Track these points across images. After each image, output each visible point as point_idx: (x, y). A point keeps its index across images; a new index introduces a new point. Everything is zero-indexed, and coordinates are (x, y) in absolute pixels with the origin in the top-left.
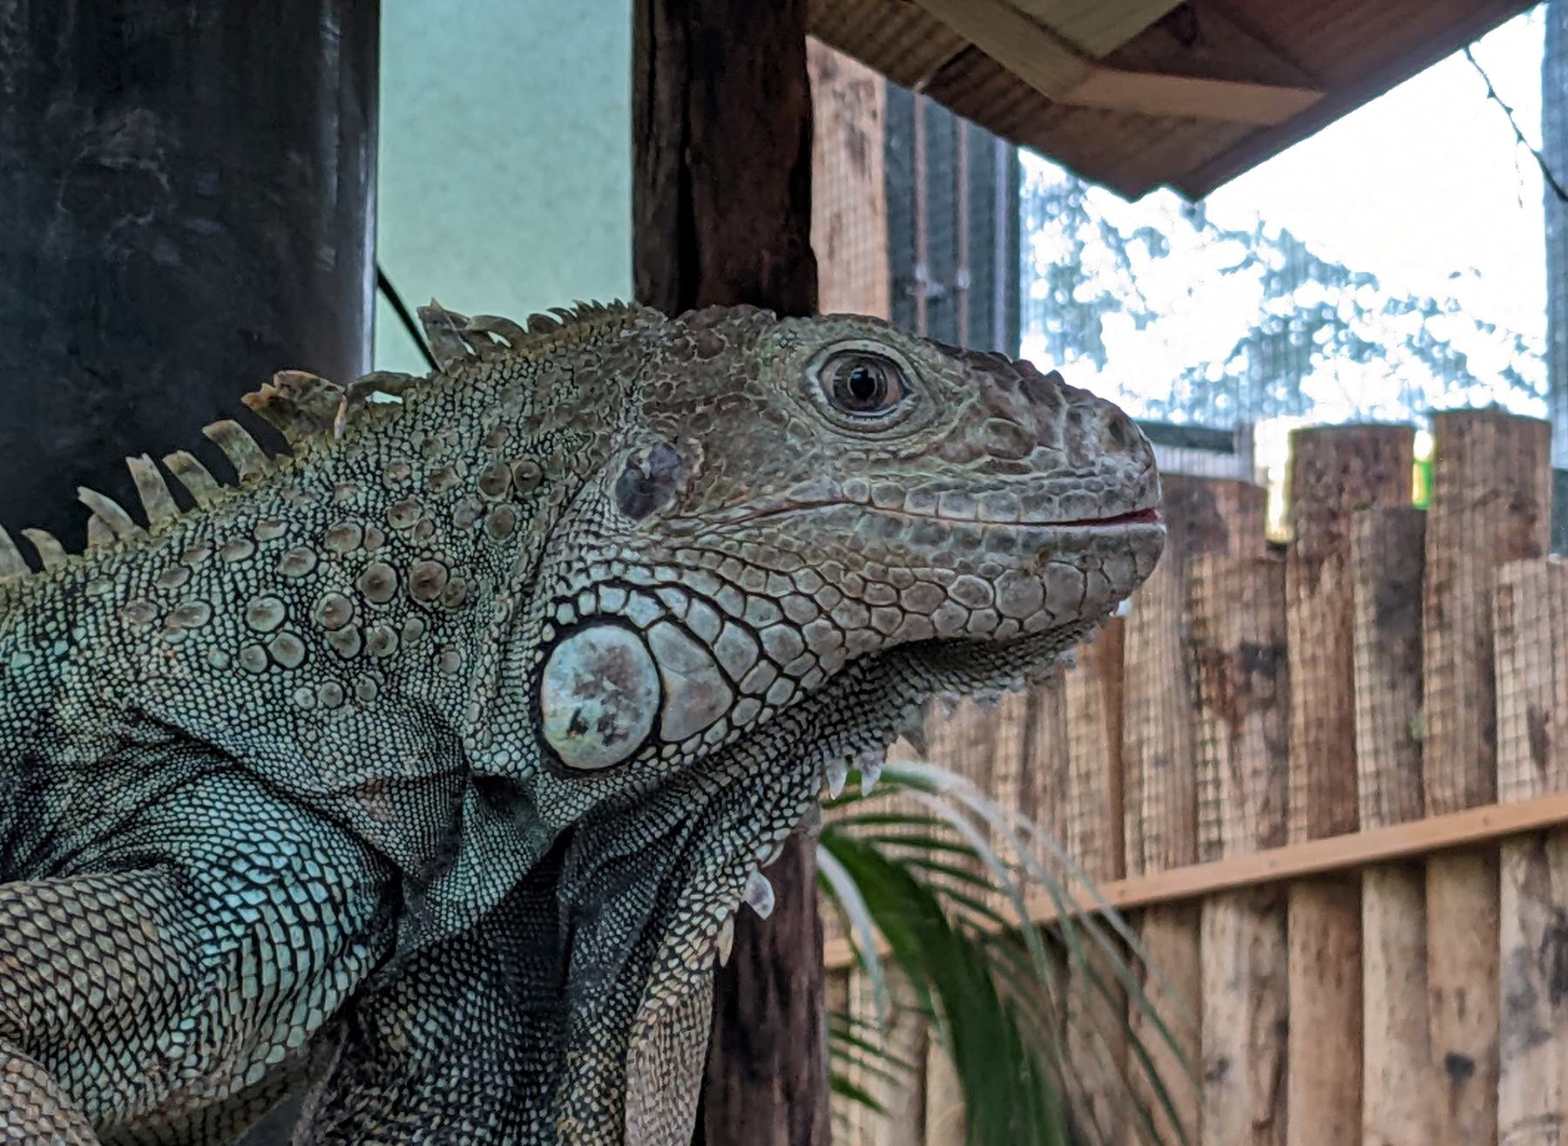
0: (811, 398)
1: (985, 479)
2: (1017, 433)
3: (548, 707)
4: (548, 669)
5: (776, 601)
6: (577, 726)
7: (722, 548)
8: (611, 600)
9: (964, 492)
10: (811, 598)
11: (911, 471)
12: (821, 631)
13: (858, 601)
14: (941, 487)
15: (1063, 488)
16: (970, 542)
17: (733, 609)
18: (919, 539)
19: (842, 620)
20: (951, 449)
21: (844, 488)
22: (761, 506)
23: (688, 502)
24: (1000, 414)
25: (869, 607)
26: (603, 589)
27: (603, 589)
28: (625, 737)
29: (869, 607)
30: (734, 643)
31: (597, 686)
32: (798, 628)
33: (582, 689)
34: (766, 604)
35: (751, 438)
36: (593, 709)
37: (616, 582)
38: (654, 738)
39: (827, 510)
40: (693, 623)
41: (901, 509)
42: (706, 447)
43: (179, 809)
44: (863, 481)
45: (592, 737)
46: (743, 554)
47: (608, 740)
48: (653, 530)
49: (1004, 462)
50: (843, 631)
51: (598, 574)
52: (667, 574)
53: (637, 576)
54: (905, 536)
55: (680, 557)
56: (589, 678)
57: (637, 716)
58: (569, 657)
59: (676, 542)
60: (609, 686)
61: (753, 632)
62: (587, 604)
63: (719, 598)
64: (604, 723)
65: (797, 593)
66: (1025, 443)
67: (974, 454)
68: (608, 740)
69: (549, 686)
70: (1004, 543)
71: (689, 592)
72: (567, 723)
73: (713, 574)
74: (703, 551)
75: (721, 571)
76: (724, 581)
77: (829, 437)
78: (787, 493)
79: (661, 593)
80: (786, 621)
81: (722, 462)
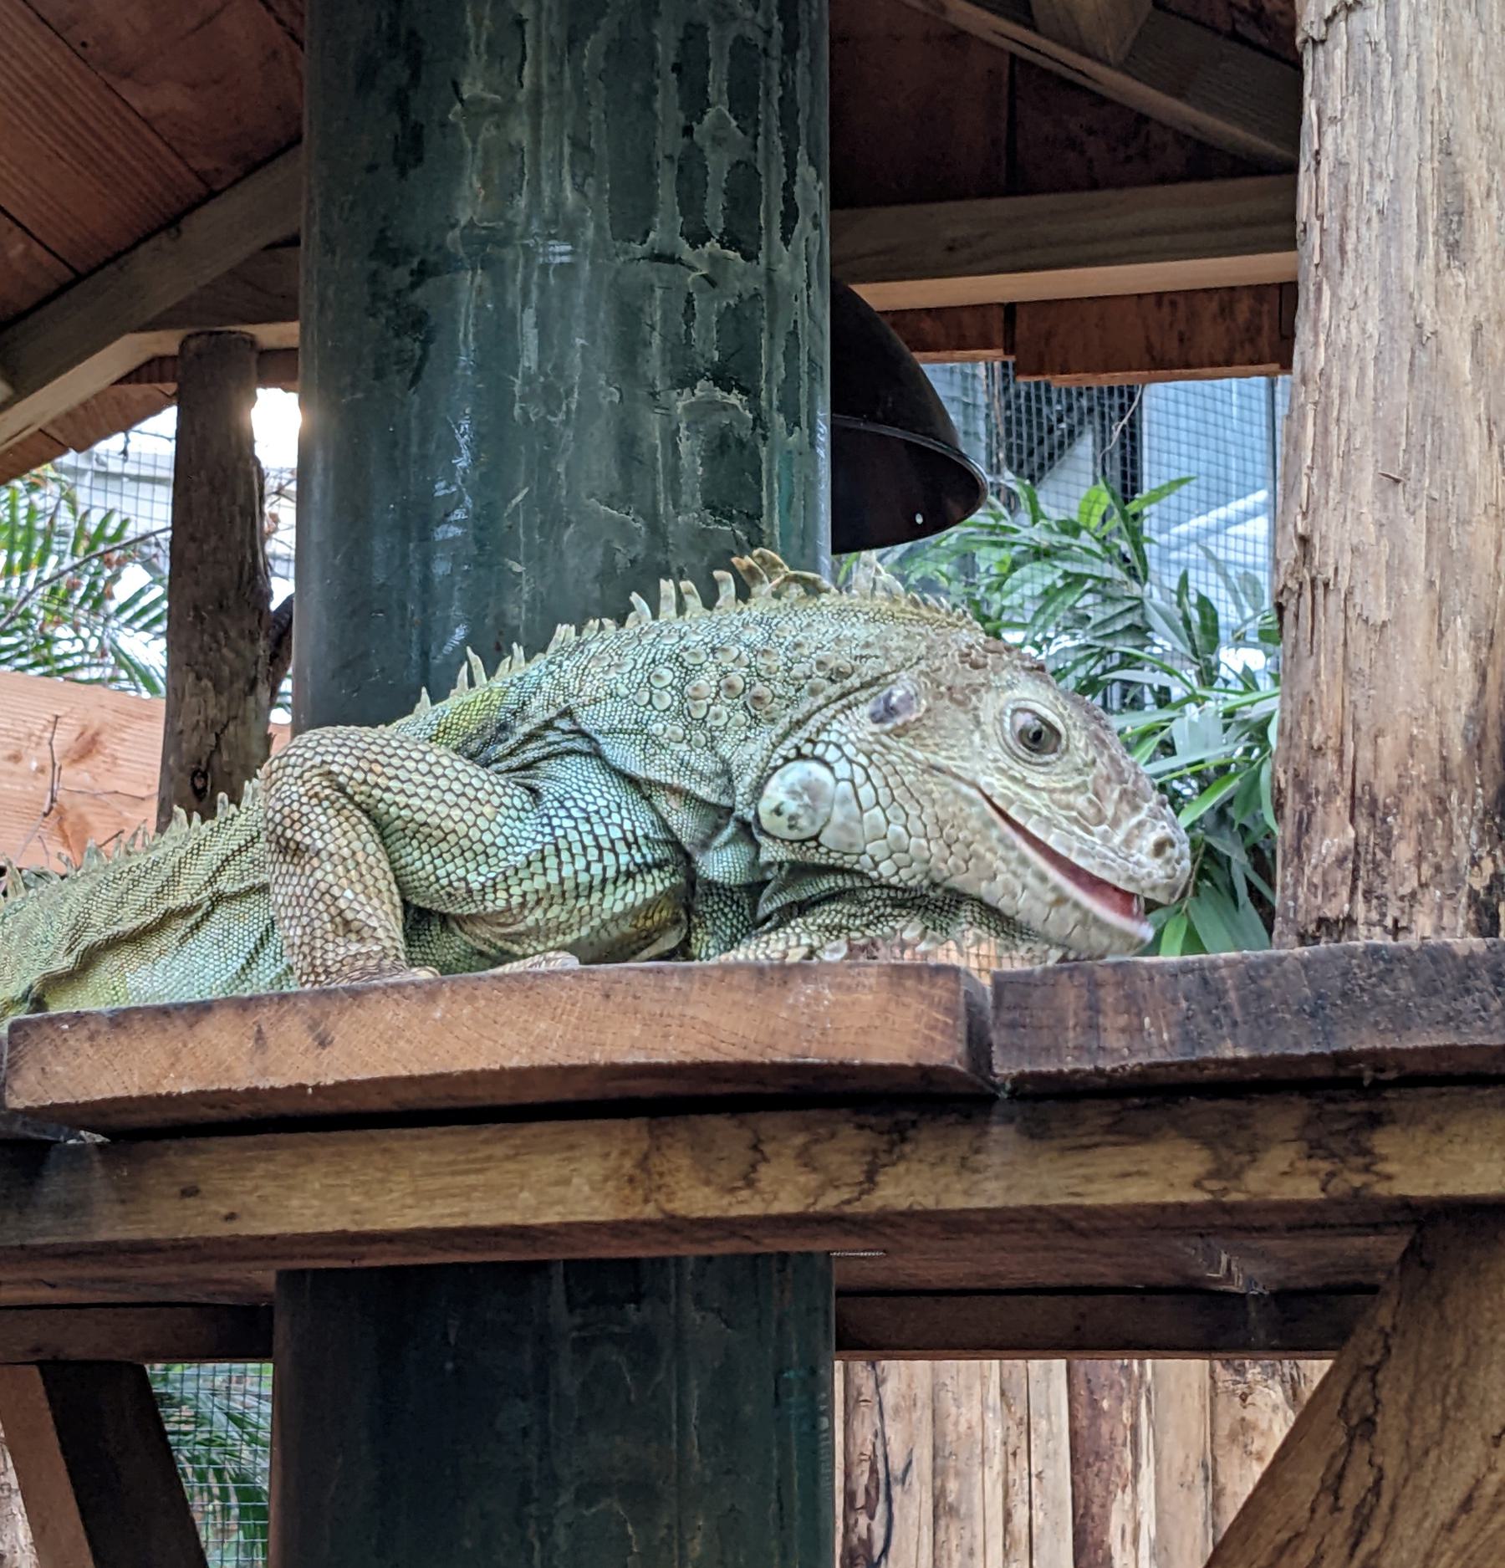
0: (1001, 721)
3: (768, 791)
4: (780, 772)
6: (778, 811)
7: (898, 768)
17: (884, 801)
21: (983, 780)
22: (933, 759)
23: (899, 732)
31: (800, 796)
33: (793, 793)
35: (955, 720)
36: (791, 806)
40: (861, 792)
42: (928, 710)
43: (553, 767)
45: (783, 821)
46: (907, 779)
47: (791, 827)
48: (873, 734)
52: (863, 760)
55: (875, 757)
56: (798, 789)
57: (813, 823)
58: (796, 772)
59: (878, 748)
60: (806, 798)
63: (880, 791)
64: (792, 818)
68: (791, 827)
69: (774, 781)
71: (868, 778)
72: (773, 805)
73: (885, 778)
74: (888, 763)
75: (890, 780)
76: (887, 785)
78: (951, 763)
79: (855, 767)
81: (930, 723)
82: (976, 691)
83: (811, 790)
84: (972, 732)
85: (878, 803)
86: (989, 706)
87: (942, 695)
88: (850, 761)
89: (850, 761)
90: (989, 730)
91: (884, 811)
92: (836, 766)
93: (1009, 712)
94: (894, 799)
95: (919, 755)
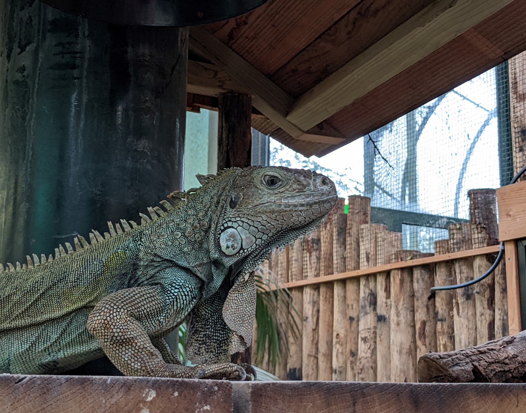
1: (297, 194)
2: (303, 185)
5: (259, 222)
6: (228, 247)
8: (230, 224)
9: (293, 197)
10: (266, 220)
11: (283, 195)
12: (269, 226)
13: (275, 220)
14: (288, 197)
15: (313, 194)
16: (295, 206)
17: (251, 224)
18: (285, 207)
19: (273, 224)
20: (290, 189)
24: (299, 182)
25: (278, 221)
26: (228, 222)
27: (228, 222)
28: (236, 248)
29: (278, 221)
30: (252, 230)
31: (230, 239)
32: (265, 226)
34: (258, 222)
36: (230, 244)
37: (230, 221)
38: (242, 248)
39: (267, 204)
41: (281, 202)
42: (243, 195)
44: (273, 198)
45: (231, 249)
47: (234, 249)
49: (301, 191)
50: (274, 225)
51: (227, 220)
53: (233, 220)
54: (282, 207)
55: (240, 216)
57: (238, 244)
59: (239, 213)
61: (257, 228)
62: (226, 225)
63: (248, 222)
64: (232, 246)
65: (263, 220)
66: (305, 186)
67: (295, 190)
70: (302, 205)
71: (243, 222)
72: (225, 247)
73: (247, 218)
76: (249, 219)
77: (266, 190)
80: (262, 225)
81: (246, 197)
82: (250, 182)
83: (232, 236)
84: (258, 191)
85: (250, 225)
86: (257, 181)
87: (243, 189)
88: (236, 222)
89: (236, 222)
90: (262, 187)
91: (253, 226)
92: (233, 225)
93: (263, 180)
94: (253, 221)
95: (250, 207)
